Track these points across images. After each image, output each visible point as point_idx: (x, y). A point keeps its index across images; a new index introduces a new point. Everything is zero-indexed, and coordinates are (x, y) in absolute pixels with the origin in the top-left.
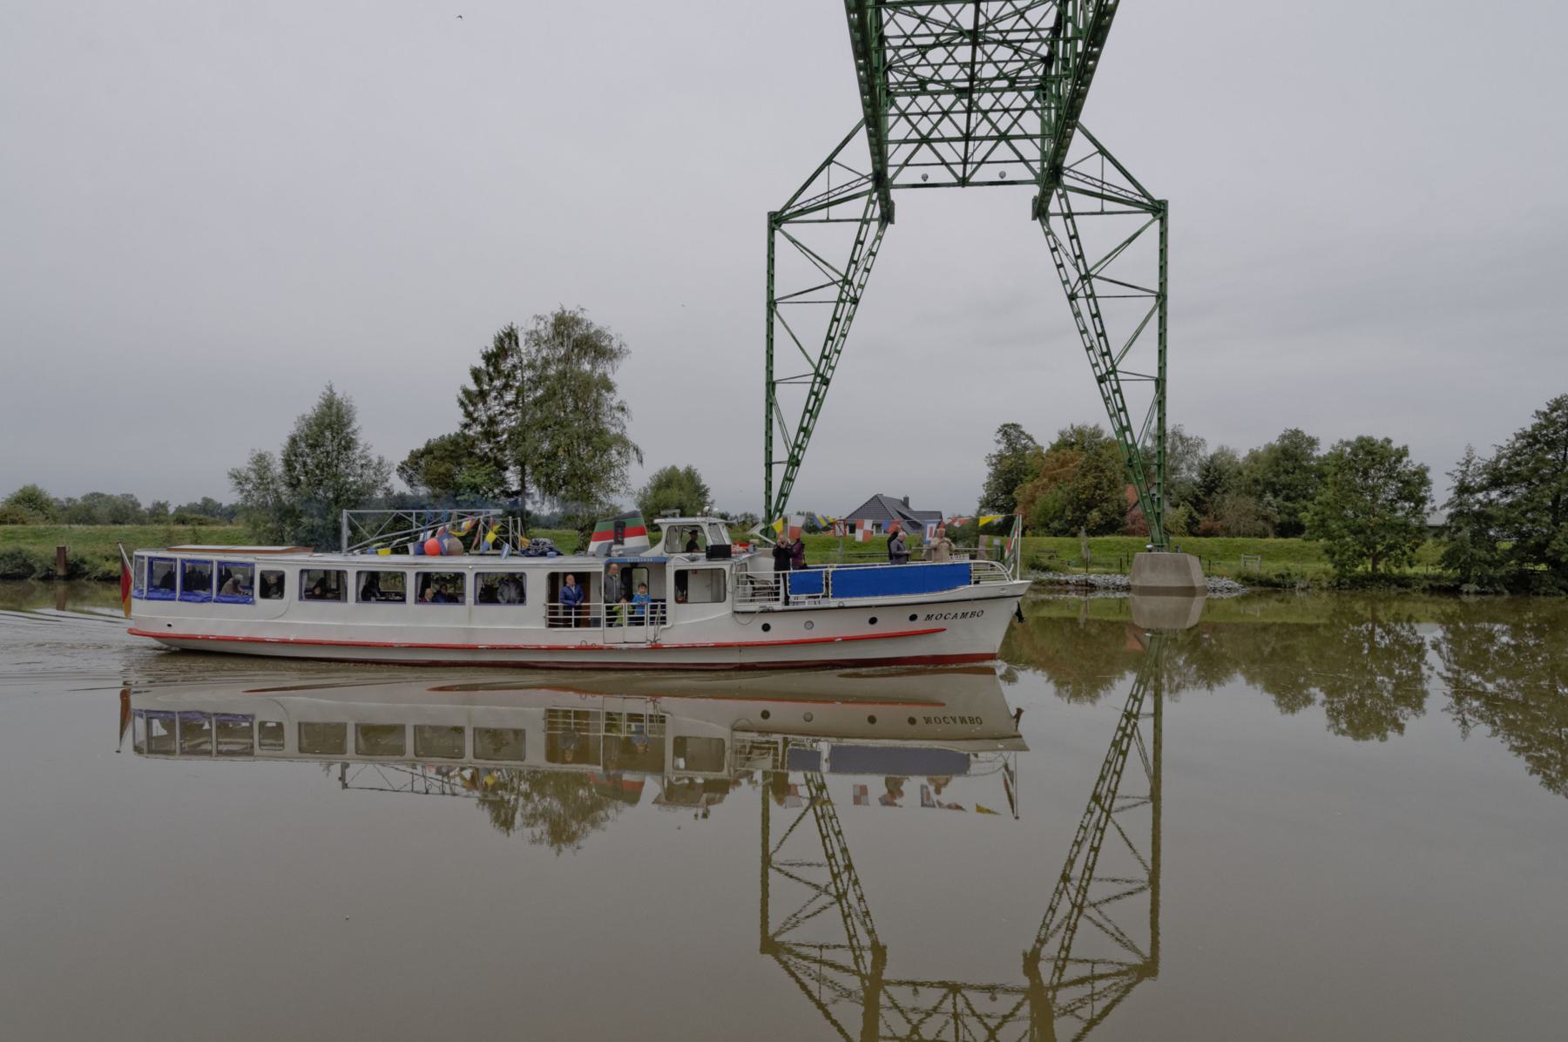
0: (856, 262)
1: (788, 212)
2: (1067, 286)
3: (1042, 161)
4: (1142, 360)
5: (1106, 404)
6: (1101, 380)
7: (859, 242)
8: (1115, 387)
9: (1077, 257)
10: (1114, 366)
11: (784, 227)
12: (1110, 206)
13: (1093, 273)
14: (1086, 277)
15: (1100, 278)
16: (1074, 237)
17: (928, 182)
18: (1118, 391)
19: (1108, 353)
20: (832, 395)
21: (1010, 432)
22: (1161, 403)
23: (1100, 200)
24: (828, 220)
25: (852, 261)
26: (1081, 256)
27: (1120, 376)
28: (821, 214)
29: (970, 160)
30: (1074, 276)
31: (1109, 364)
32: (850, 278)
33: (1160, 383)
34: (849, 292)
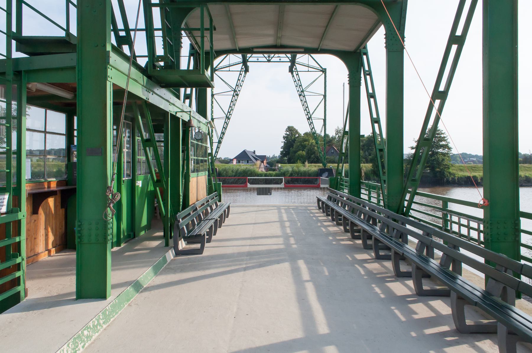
0: (238, 86)
1: (217, 68)
2: (299, 92)
3: (291, 57)
4: (319, 114)
5: (310, 126)
6: (308, 119)
7: (239, 80)
8: (311, 122)
9: (300, 86)
10: (311, 116)
11: (216, 72)
12: (310, 69)
13: (304, 90)
14: (302, 91)
15: (306, 91)
16: (299, 80)
17: (259, 61)
18: (312, 123)
19: (309, 112)
20: (231, 122)
21: (290, 129)
22: (325, 125)
23: (308, 67)
24: (229, 71)
25: (237, 85)
26: (301, 85)
27: (312, 118)
28: (227, 69)
29: (270, 56)
30: (300, 91)
31: (309, 116)
32: (236, 90)
33: (325, 120)
34: (236, 93)
